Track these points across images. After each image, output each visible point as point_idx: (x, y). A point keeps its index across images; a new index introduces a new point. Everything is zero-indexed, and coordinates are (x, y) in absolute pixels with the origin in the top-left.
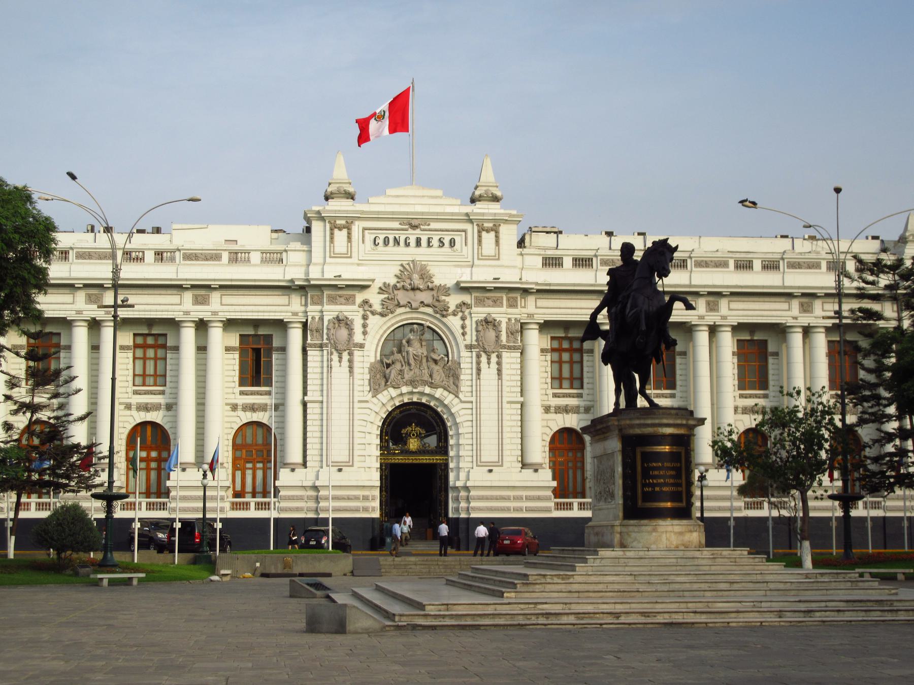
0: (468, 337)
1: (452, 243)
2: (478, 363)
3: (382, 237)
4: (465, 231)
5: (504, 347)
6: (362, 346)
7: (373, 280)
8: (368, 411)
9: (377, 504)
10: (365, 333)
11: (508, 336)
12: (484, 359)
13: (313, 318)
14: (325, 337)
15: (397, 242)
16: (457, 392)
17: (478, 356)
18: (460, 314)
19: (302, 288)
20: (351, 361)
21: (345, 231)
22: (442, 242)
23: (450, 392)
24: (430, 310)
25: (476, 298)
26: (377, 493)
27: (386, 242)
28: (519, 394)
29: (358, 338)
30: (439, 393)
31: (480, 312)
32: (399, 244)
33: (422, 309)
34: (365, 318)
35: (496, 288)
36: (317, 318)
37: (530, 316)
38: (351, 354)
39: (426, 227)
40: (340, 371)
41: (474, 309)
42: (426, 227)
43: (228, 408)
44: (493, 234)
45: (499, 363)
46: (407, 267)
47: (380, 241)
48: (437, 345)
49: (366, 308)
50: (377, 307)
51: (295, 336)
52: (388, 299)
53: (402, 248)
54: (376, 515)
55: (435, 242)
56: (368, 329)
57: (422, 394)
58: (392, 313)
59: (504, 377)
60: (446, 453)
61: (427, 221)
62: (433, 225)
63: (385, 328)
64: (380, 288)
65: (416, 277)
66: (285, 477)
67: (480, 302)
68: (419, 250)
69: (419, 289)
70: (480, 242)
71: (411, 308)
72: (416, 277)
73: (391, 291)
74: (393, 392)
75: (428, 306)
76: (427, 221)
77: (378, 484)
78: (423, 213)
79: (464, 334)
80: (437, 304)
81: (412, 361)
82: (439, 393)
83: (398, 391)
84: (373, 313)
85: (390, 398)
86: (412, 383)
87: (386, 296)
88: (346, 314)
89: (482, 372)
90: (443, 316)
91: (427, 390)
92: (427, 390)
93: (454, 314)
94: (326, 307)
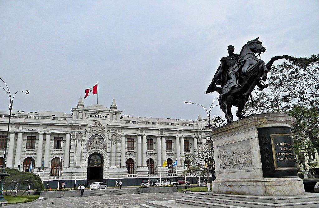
1: (106, 117)
2: (111, 144)
3: (90, 115)
6: (84, 140)
7: (88, 124)
10: (85, 136)
12: (113, 143)
13: (73, 133)
17: (111, 142)
18: (107, 133)
19: (70, 126)
20: (81, 143)
24: (100, 132)
29: (83, 138)
30: (102, 150)
31: (111, 133)
33: (99, 132)
38: (82, 141)
40: (79, 145)
43: (51, 154)
44: (115, 115)
47: (90, 116)
48: (102, 140)
51: (68, 137)
53: (94, 118)
59: (117, 147)
60: (103, 164)
62: (102, 113)
63: (90, 135)
65: (97, 124)
66: (64, 170)
68: (98, 118)
69: (98, 127)
75: (100, 131)
79: (108, 137)
82: (102, 150)
83: (92, 150)
84: (87, 132)
85: (90, 152)
86: (96, 148)
90: (104, 133)
91: (99, 150)
92: (99, 150)
94: (76, 130)
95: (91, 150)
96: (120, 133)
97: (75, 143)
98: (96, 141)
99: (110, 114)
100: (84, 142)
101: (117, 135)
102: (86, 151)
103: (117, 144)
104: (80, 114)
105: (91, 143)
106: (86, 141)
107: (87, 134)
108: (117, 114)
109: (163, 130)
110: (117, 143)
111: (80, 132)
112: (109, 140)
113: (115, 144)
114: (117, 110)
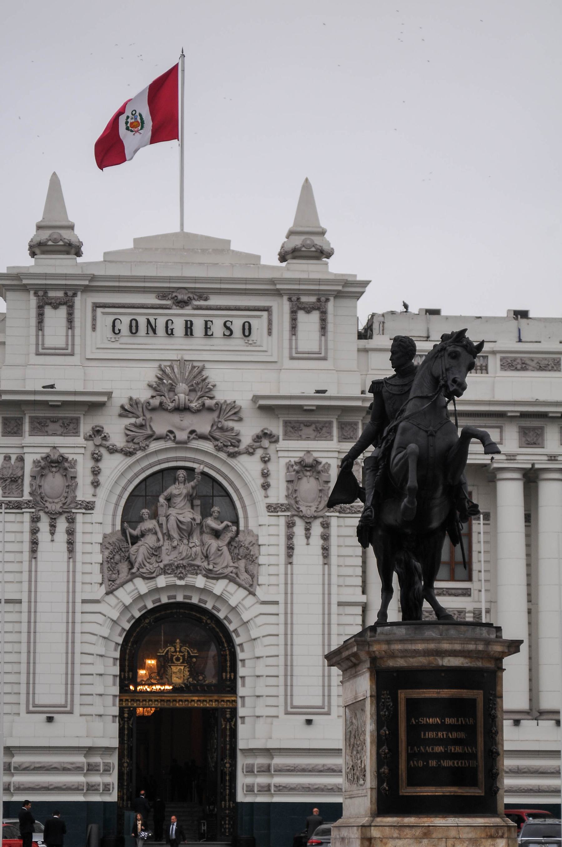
0: (271, 492)
1: (247, 331)
3: (126, 320)
4: (267, 309)
6: (89, 507)
7: (109, 394)
8: (100, 619)
9: (113, 779)
10: (96, 484)
12: (299, 529)
14: (27, 489)
15: (152, 328)
16: (251, 585)
17: (290, 525)
18: (259, 453)
20: (71, 533)
21: (63, 311)
22: (228, 328)
23: (240, 585)
24: (208, 446)
25: (286, 423)
26: (114, 760)
27: (134, 329)
28: (360, 590)
29: (84, 492)
30: (218, 587)
31: (291, 450)
32: (154, 331)
33: (196, 444)
34: (97, 459)
35: (319, 407)
36: (14, 458)
38: (71, 521)
39: (202, 303)
40: (53, 548)
41: (283, 444)
42: (202, 303)
44: (315, 316)
45: (325, 537)
46: (168, 370)
47: (124, 326)
49: (98, 440)
52: (135, 425)
54: (113, 797)
55: (217, 328)
56: (101, 478)
57: (193, 588)
58: (144, 449)
59: (334, 559)
60: (233, 690)
61: (203, 295)
62: (214, 301)
64: (122, 407)
65: (182, 387)
67: (293, 429)
70: (294, 328)
71: (175, 440)
72: (182, 387)
73: (140, 413)
74: (142, 586)
76: (203, 295)
77: (115, 743)
78: (195, 280)
79: (266, 486)
80: (217, 434)
83: (151, 585)
84: (112, 450)
85: (135, 594)
87: (133, 420)
88: (62, 451)
89: (296, 552)
90: (233, 455)
91: (200, 581)
92: (200, 581)
93: (250, 452)
94: (28, 439)
95: (139, 582)
97: (27, 537)
98: (172, 512)
99: (282, 308)
100: (88, 528)
102: (103, 590)
104: (55, 318)
105: (135, 533)
106: (99, 524)
107: (112, 465)
108: (330, 306)
109: (543, 416)
110: (334, 531)
111: (54, 456)
112: (272, 509)
113: (316, 541)
114: (336, 266)
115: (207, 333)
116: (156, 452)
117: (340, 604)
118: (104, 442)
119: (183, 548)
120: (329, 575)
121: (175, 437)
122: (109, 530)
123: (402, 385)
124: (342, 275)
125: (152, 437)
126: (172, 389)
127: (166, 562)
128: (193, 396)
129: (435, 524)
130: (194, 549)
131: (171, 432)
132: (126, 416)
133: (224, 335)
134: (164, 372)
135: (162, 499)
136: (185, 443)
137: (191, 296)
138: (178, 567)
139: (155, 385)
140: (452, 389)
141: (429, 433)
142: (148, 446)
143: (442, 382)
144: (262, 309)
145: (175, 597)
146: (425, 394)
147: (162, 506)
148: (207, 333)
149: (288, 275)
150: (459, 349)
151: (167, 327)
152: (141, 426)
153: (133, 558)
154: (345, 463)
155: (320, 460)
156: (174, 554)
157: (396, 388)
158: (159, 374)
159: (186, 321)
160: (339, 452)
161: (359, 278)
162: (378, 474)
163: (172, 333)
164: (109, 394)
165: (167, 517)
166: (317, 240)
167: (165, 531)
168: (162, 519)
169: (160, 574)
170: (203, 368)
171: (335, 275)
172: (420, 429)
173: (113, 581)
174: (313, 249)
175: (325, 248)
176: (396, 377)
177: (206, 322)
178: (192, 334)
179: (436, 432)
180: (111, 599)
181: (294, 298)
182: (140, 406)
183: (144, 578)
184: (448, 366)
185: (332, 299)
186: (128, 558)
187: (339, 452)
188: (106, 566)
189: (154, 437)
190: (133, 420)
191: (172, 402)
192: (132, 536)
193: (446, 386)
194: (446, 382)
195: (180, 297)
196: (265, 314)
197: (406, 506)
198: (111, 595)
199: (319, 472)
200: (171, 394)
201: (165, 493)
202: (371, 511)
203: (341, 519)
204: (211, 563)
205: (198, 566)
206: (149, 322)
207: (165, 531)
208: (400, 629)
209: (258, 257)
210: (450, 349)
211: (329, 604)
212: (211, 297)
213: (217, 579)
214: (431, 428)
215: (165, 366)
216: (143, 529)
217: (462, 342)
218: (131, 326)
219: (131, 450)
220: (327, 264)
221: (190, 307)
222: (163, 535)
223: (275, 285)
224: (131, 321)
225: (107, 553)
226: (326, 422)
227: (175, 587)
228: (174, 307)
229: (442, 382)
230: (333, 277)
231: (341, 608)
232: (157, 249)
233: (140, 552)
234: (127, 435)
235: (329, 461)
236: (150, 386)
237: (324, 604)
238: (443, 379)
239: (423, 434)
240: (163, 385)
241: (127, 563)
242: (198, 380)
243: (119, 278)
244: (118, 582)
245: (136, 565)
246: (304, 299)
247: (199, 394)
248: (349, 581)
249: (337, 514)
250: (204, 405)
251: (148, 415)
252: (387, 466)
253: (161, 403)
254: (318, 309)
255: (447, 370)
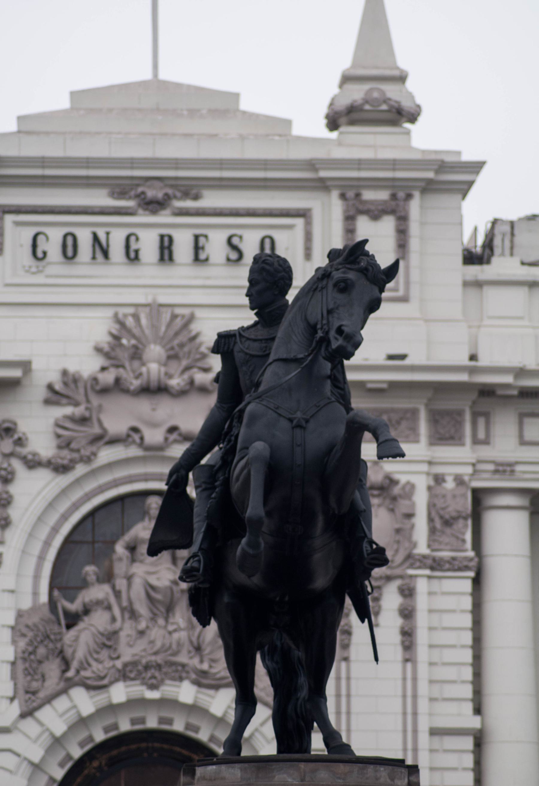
3: (55, 236)
4: (304, 214)
5: (422, 562)
7: (26, 366)
11: (432, 531)
15: (101, 249)
22: (235, 248)
27: (70, 250)
28: (469, 707)
32: (106, 254)
35: (394, 385)
37: (504, 469)
39: (189, 204)
42: (189, 204)
46: (130, 322)
47: (52, 245)
50: (42, 444)
52: (71, 419)
53: (117, 270)
58: (88, 460)
59: (422, 652)
61: (190, 189)
62: (211, 200)
63: (64, 506)
64: (50, 387)
65: (155, 351)
71: (141, 444)
72: (155, 351)
73: (81, 397)
74: (84, 702)
76: (190, 189)
78: (176, 164)
81: (142, 608)
83: (101, 699)
84: (33, 463)
87: (69, 410)
91: (186, 692)
92: (186, 692)
96: (459, 459)
98: (139, 570)
101: (421, 500)
102: (15, 709)
103: (422, 620)
105: (74, 607)
108: (415, 207)
110: (422, 602)
114: (425, 137)
115: (198, 255)
116: (110, 466)
117: (434, 732)
118: (18, 449)
119: (157, 634)
120: (415, 679)
121: (142, 439)
122: (26, 604)
123: (267, 340)
124: (436, 152)
125: (103, 439)
126: (137, 354)
127: (127, 657)
128: (175, 367)
129: (321, 582)
130: (176, 636)
131: (135, 430)
132: (57, 403)
133: (228, 260)
134: (122, 324)
135: (120, 549)
136: (160, 448)
137: (170, 191)
138: (147, 667)
139: (106, 348)
140: (335, 345)
141: (295, 422)
142: (94, 454)
143: (320, 334)
144: (97, 210)
145: (142, 721)
146: (292, 356)
147: (120, 559)
148: (198, 255)
149: (339, 153)
150: (351, 275)
151: (127, 246)
152: (83, 420)
153: (68, 652)
154: (174, 477)
155: (396, 477)
156: (141, 646)
157: (256, 345)
158: (115, 328)
159: (162, 237)
160: (430, 463)
161: (466, 157)
162: (213, 496)
163: (137, 258)
164: (26, 366)
165: (129, 578)
166: (391, 91)
167: (125, 603)
168: (121, 584)
169: (117, 680)
170: (191, 318)
171: (424, 152)
172: (280, 415)
173: (34, 693)
174: (384, 107)
175: (406, 104)
176: (259, 326)
177: (197, 238)
178: (171, 259)
179: (307, 421)
180: (29, 726)
181: (351, 194)
182: (81, 385)
183: (89, 688)
184: (331, 306)
185: (417, 194)
186: (61, 652)
187: (430, 463)
188: (20, 666)
189: (106, 439)
190: (69, 410)
191: (137, 377)
192: (67, 613)
193: (325, 340)
194: (327, 333)
195: (150, 194)
196: (299, 222)
197: (244, 554)
198: (29, 721)
199: (394, 499)
200: (136, 364)
201: (128, 537)
202: (199, 561)
203: (435, 582)
204: (206, 659)
205: (184, 666)
206: (96, 238)
207: (125, 603)
208: (231, 770)
209: (288, 123)
210: (337, 275)
211: (415, 731)
212: (206, 193)
213: (216, 688)
214: (299, 415)
215: (125, 316)
216: (87, 600)
217: (359, 263)
218: (64, 246)
219: (65, 462)
220: (408, 133)
221: (167, 211)
222: (123, 610)
223: (316, 170)
224: (65, 236)
225: (22, 644)
226: (406, 411)
227: (142, 702)
228: (140, 211)
229: (320, 334)
230: (418, 156)
231: (436, 739)
232: (110, 110)
233: (80, 640)
234: (58, 436)
235: (413, 479)
236: (98, 350)
237: (405, 731)
238: (321, 328)
239: (284, 424)
240: (122, 348)
241: (58, 661)
242: (183, 338)
243: (43, 162)
244: (42, 695)
245: (75, 665)
246: (368, 195)
247: (185, 363)
248: (451, 691)
249: (427, 572)
250: (192, 382)
251: (95, 401)
252: (227, 483)
253: (118, 381)
254: (393, 212)
255: (329, 312)
